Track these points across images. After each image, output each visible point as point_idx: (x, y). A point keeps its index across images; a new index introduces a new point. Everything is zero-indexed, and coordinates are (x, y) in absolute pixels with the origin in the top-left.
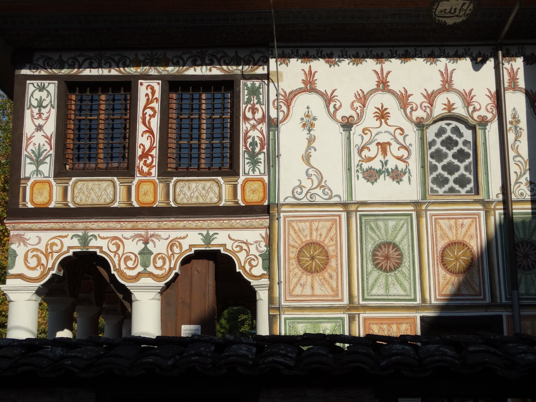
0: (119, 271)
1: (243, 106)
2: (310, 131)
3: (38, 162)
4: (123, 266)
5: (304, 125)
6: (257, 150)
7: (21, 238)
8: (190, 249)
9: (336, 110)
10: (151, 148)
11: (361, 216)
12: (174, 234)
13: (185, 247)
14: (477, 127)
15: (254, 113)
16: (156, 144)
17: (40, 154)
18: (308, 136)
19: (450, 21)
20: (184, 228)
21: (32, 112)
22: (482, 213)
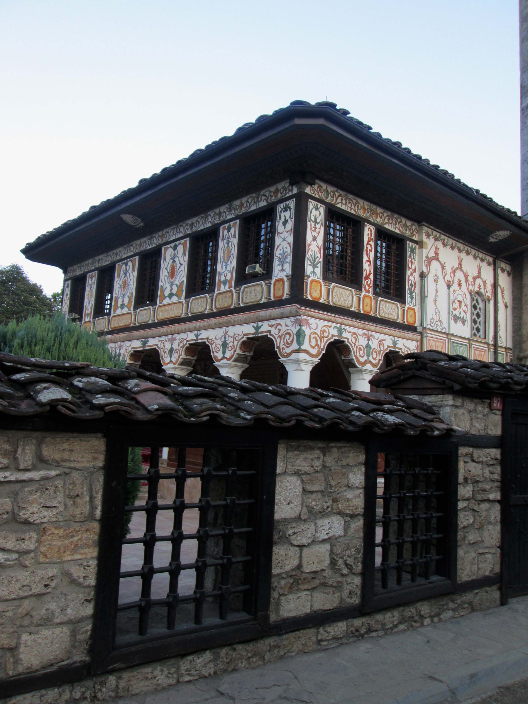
0: (356, 356)
1: (408, 258)
2: (436, 284)
3: (314, 266)
4: (358, 355)
5: (435, 281)
6: (413, 290)
7: (307, 322)
8: (387, 349)
9: (445, 275)
10: (370, 274)
11: (453, 342)
12: (382, 337)
13: (386, 347)
14: (487, 302)
15: (412, 265)
16: (372, 272)
17: (315, 260)
18: (435, 288)
19: (491, 240)
20: (385, 334)
21: (311, 224)
22: (487, 349)
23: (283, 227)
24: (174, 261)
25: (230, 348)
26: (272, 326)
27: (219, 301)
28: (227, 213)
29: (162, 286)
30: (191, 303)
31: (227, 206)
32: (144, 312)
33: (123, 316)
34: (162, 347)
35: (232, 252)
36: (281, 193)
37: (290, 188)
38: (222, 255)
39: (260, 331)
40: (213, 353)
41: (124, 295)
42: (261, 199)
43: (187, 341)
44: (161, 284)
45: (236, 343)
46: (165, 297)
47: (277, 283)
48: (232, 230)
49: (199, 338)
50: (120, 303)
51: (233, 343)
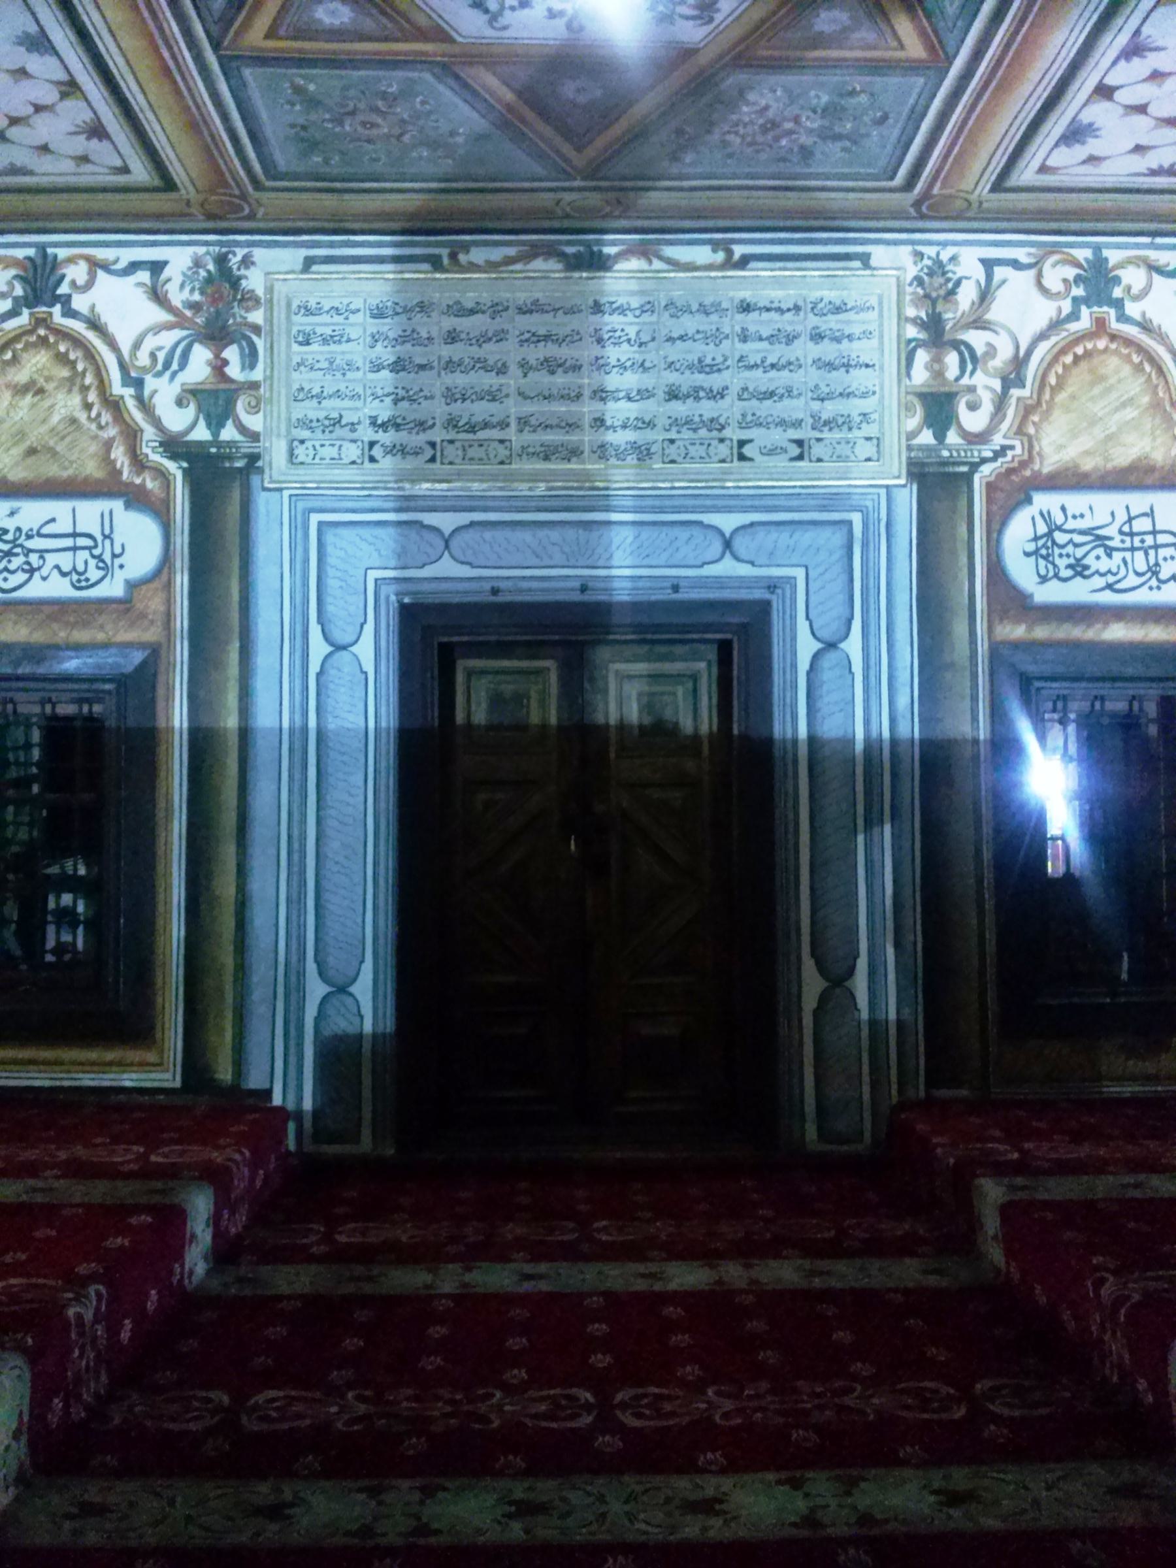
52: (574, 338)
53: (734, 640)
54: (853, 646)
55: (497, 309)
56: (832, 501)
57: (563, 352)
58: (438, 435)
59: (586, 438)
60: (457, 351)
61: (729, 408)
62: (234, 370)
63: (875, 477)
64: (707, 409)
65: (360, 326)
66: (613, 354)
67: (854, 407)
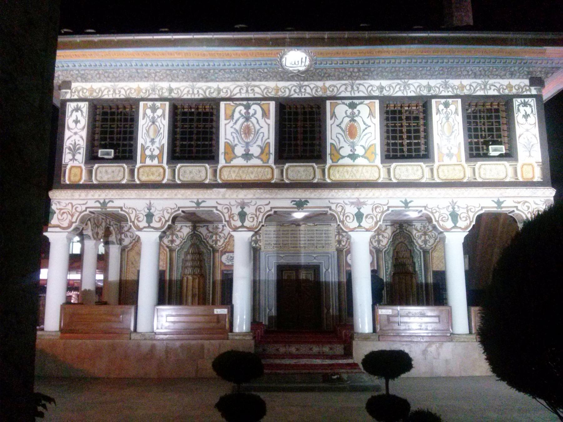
23: (524, 119)
24: (353, 120)
25: (464, 219)
26: (519, 203)
27: (443, 171)
28: (441, 89)
29: (332, 144)
30: (395, 169)
31: (439, 81)
32: (301, 169)
33: (251, 169)
34: (339, 209)
35: (456, 127)
36: (515, 89)
37: (528, 88)
38: (440, 128)
39: (502, 205)
40: (438, 222)
41: (247, 144)
42: (490, 89)
43: (389, 207)
44: (329, 141)
45: (471, 215)
46: (343, 157)
47: (525, 167)
48: (452, 108)
49: (409, 205)
50: (239, 150)
51: (468, 214)
52: (297, 234)
53: (316, 269)
54: (330, 270)
55: (288, 231)
56: (328, 253)
57: (295, 236)
58: (281, 245)
59: (298, 245)
60: (283, 236)
61: (315, 242)
62: (258, 238)
63: (332, 249)
64: (312, 242)
65: (273, 232)
66: (301, 236)
67: (329, 242)
